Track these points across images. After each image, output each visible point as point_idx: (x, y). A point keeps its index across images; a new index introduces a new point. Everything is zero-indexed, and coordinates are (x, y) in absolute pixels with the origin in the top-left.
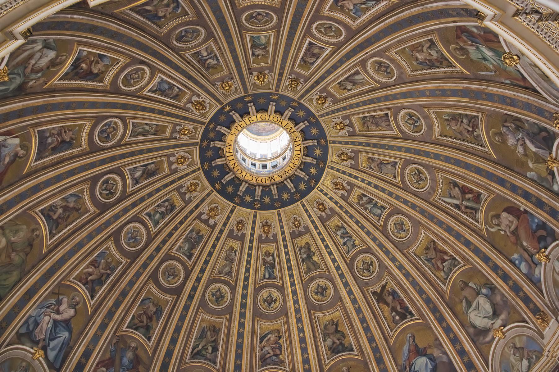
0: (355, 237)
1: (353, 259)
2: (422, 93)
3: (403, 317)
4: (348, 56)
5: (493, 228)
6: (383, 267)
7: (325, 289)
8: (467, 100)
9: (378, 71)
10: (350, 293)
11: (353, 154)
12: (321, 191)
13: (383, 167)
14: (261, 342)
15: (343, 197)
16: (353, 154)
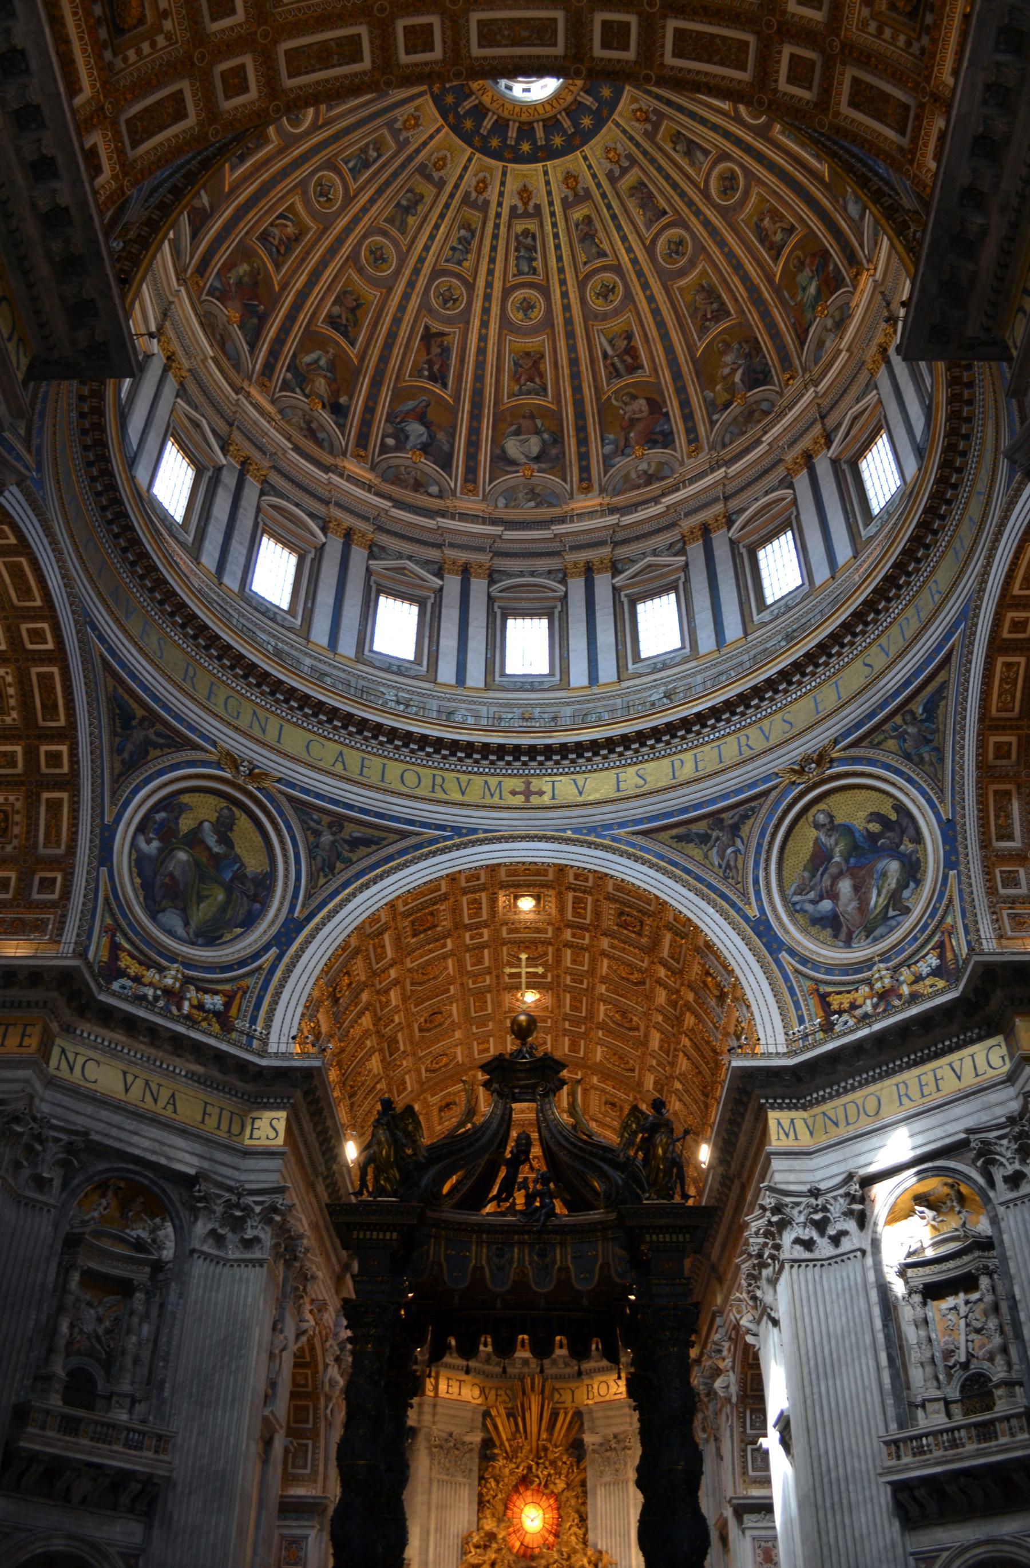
0: (472, 257)
1: (444, 273)
2: (722, 243)
3: (432, 378)
4: (727, 135)
5: (616, 400)
6: (465, 318)
7: (384, 261)
8: (745, 294)
9: (722, 178)
10: (406, 297)
11: (582, 193)
12: (504, 174)
13: (588, 242)
14: (278, 218)
15: (513, 209)
16: (582, 193)
